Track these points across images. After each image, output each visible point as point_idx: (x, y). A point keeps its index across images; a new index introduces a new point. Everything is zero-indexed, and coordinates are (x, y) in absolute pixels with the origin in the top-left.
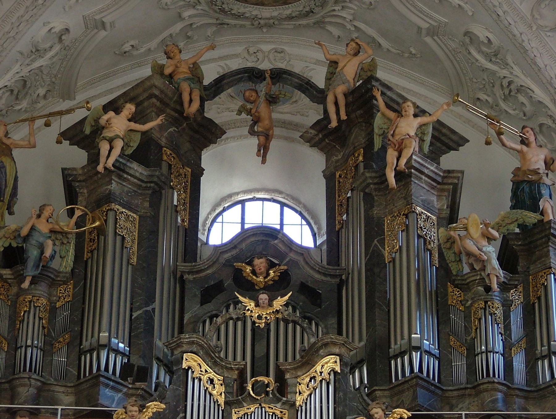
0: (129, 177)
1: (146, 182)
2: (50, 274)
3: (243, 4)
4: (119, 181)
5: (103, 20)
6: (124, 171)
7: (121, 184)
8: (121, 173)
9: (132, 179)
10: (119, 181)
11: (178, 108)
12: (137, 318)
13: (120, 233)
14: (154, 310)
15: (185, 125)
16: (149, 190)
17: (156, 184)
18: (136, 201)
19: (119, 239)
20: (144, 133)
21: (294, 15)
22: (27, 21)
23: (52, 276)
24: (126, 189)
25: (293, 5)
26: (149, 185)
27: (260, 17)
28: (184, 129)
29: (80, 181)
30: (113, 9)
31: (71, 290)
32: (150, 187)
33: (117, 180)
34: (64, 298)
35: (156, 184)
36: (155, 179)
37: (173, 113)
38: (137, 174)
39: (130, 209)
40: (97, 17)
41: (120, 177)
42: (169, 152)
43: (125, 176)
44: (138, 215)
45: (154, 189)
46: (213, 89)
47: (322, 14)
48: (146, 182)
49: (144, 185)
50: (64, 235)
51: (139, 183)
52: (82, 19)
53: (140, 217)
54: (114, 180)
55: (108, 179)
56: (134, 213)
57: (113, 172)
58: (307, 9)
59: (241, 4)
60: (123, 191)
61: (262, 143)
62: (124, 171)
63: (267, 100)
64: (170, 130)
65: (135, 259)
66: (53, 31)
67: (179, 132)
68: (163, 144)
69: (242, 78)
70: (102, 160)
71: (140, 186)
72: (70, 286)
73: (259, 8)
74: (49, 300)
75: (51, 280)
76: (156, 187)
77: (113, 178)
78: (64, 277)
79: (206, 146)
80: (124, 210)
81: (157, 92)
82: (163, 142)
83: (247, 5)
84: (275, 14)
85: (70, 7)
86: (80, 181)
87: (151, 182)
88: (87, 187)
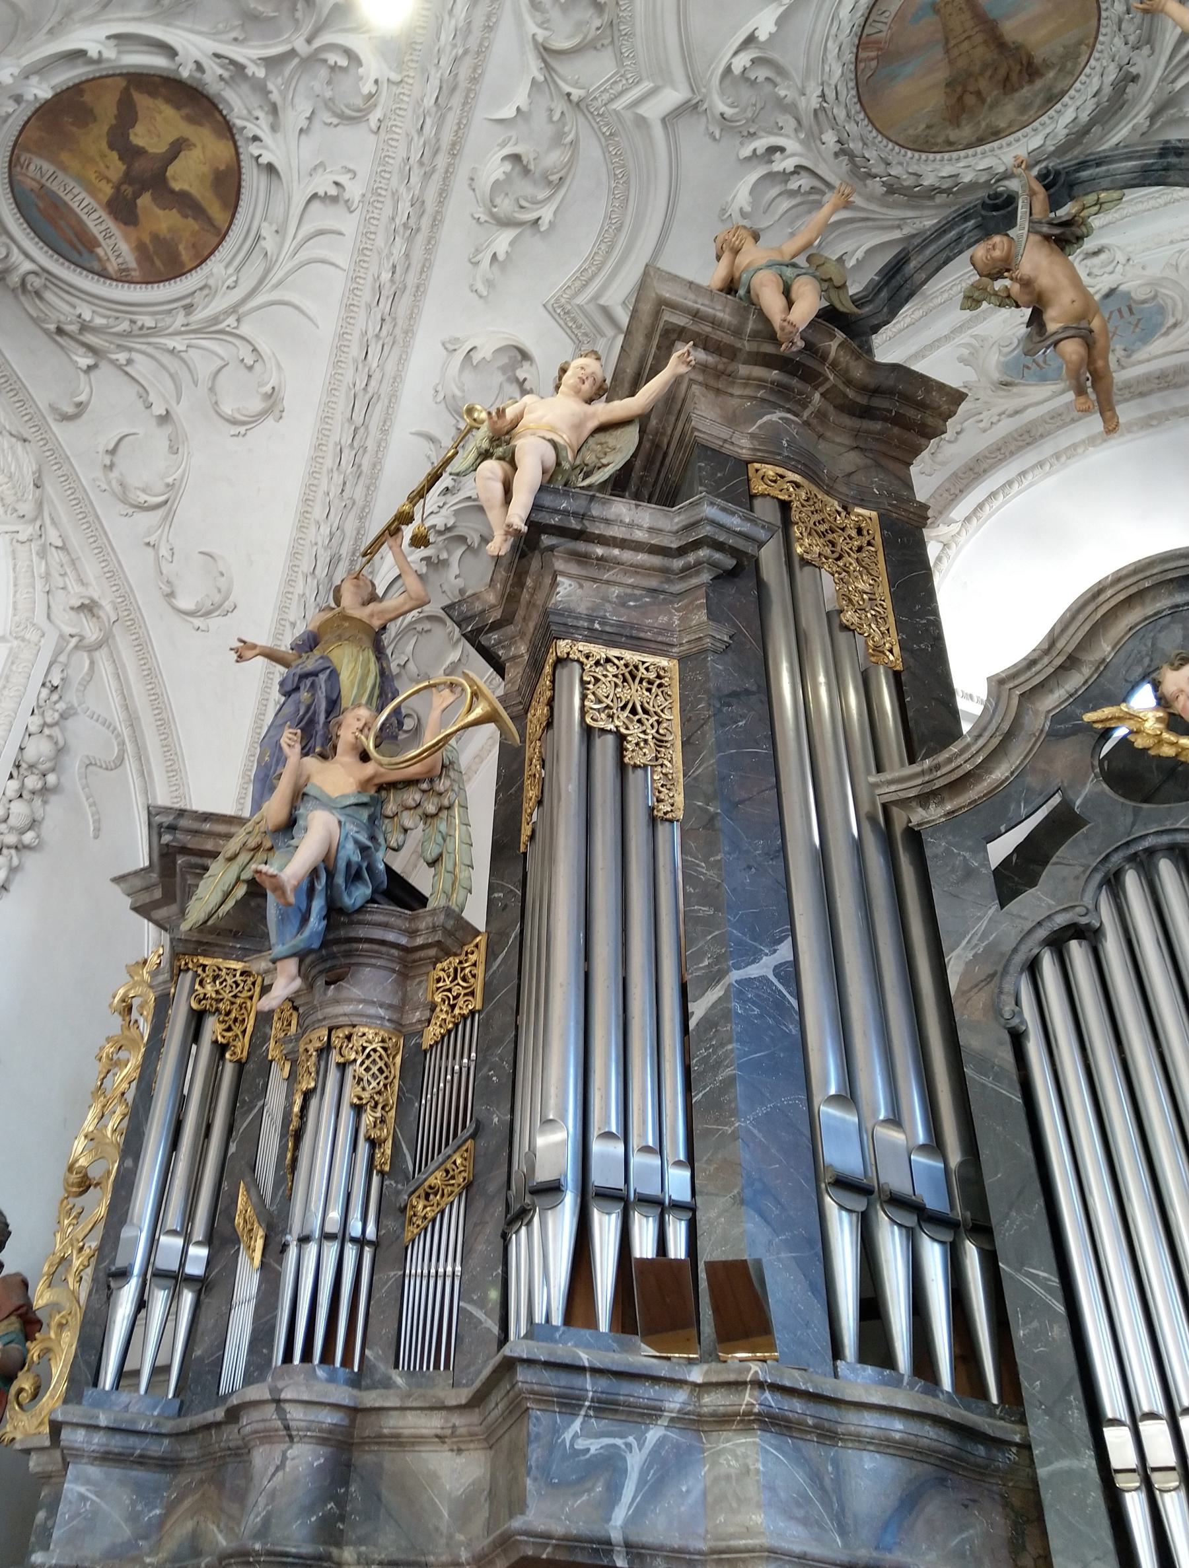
0: (616, 552)
1: (682, 551)
2: (378, 934)
3: (946, 156)
4: (584, 573)
5: (602, 302)
6: (580, 535)
7: (594, 580)
8: (581, 546)
9: (627, 556)
10: (584, 573)
11: (768, 348)
12: (708, 1022)
13: (601, 724)
14: (791, 973)
15: (817, 396)
16: (697, 573)
17: (718, 546)
18: (663, 619)
19: (605, 748)
20: (642, 420)
21: (1084, 117)
22: (377, 336)
23: (391, 937)
24: (615, 591)
25: (1072, 92)
26: (691, 558)
27: (1001, 169)
28: (821, 415)
29: (496, 626)
30: (610, 264)
31: (480, 971)
32: (698, 563)
33: (573, 568)
34: (453, 1007)
35: (718, 546)
36: (706, 530)
37: (759, 372)
38: (640, 535)
39: (636, 643)
40: (582, 299)
41: (582, 558)
42: (770, 471)
43: (600, 551)
44: (671, 657)
45: (713, 565)
46: (884, 294)
47: (1158, 73)
48: (682, 551)
49: (678, 564)
50: (425, 786)
51: (656, 560)
52: (545, 314)
53: (682, 660)
54: (563, 574)
55: (548, 581)
56: (654, 653)
57: (551, 549)
58: (1112, 75)
59: (939, 156)
60: (606, 599)
61: (1075, 357)
62: (580, 535)
63: (1047, 237)
64: (765, 419)
65: (680, 799)
66: (476, 357)
67: (806, 423)
68: (745, 454)
69: (960, 237)
70: (494, 515)
71: (665, 571)
72: (473, 958)
73: (992, 150)
74: (399, 1027)
75: (395, 952)
76: (717, 556)
77: (559, 565)
78: (434, 929)
79: (916, 451)
80: (613, 653)
81: (680, 320)
82: (743, 446)
83: (955, 155)
84: (1036, 142)
85: (490, 284)
86: (496, 626)
87: (696, 545)
88: (522, 634)
